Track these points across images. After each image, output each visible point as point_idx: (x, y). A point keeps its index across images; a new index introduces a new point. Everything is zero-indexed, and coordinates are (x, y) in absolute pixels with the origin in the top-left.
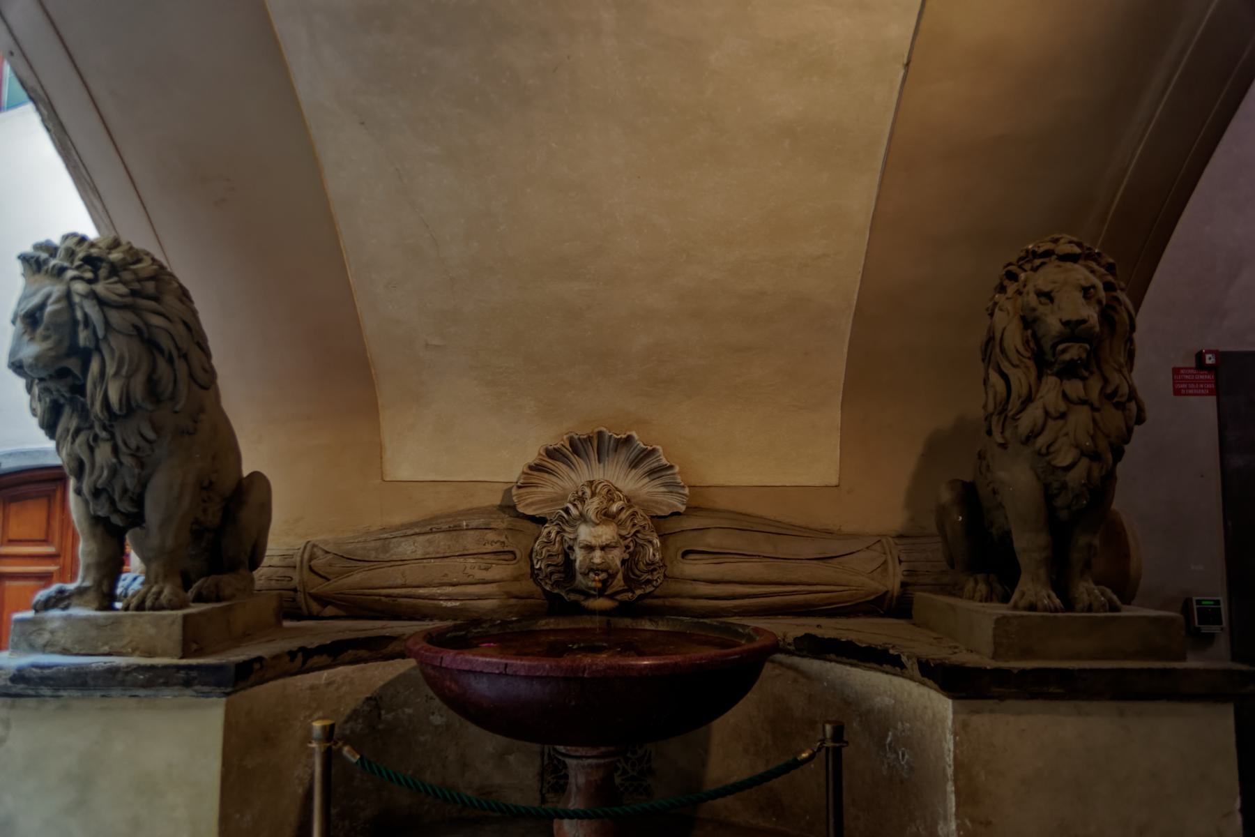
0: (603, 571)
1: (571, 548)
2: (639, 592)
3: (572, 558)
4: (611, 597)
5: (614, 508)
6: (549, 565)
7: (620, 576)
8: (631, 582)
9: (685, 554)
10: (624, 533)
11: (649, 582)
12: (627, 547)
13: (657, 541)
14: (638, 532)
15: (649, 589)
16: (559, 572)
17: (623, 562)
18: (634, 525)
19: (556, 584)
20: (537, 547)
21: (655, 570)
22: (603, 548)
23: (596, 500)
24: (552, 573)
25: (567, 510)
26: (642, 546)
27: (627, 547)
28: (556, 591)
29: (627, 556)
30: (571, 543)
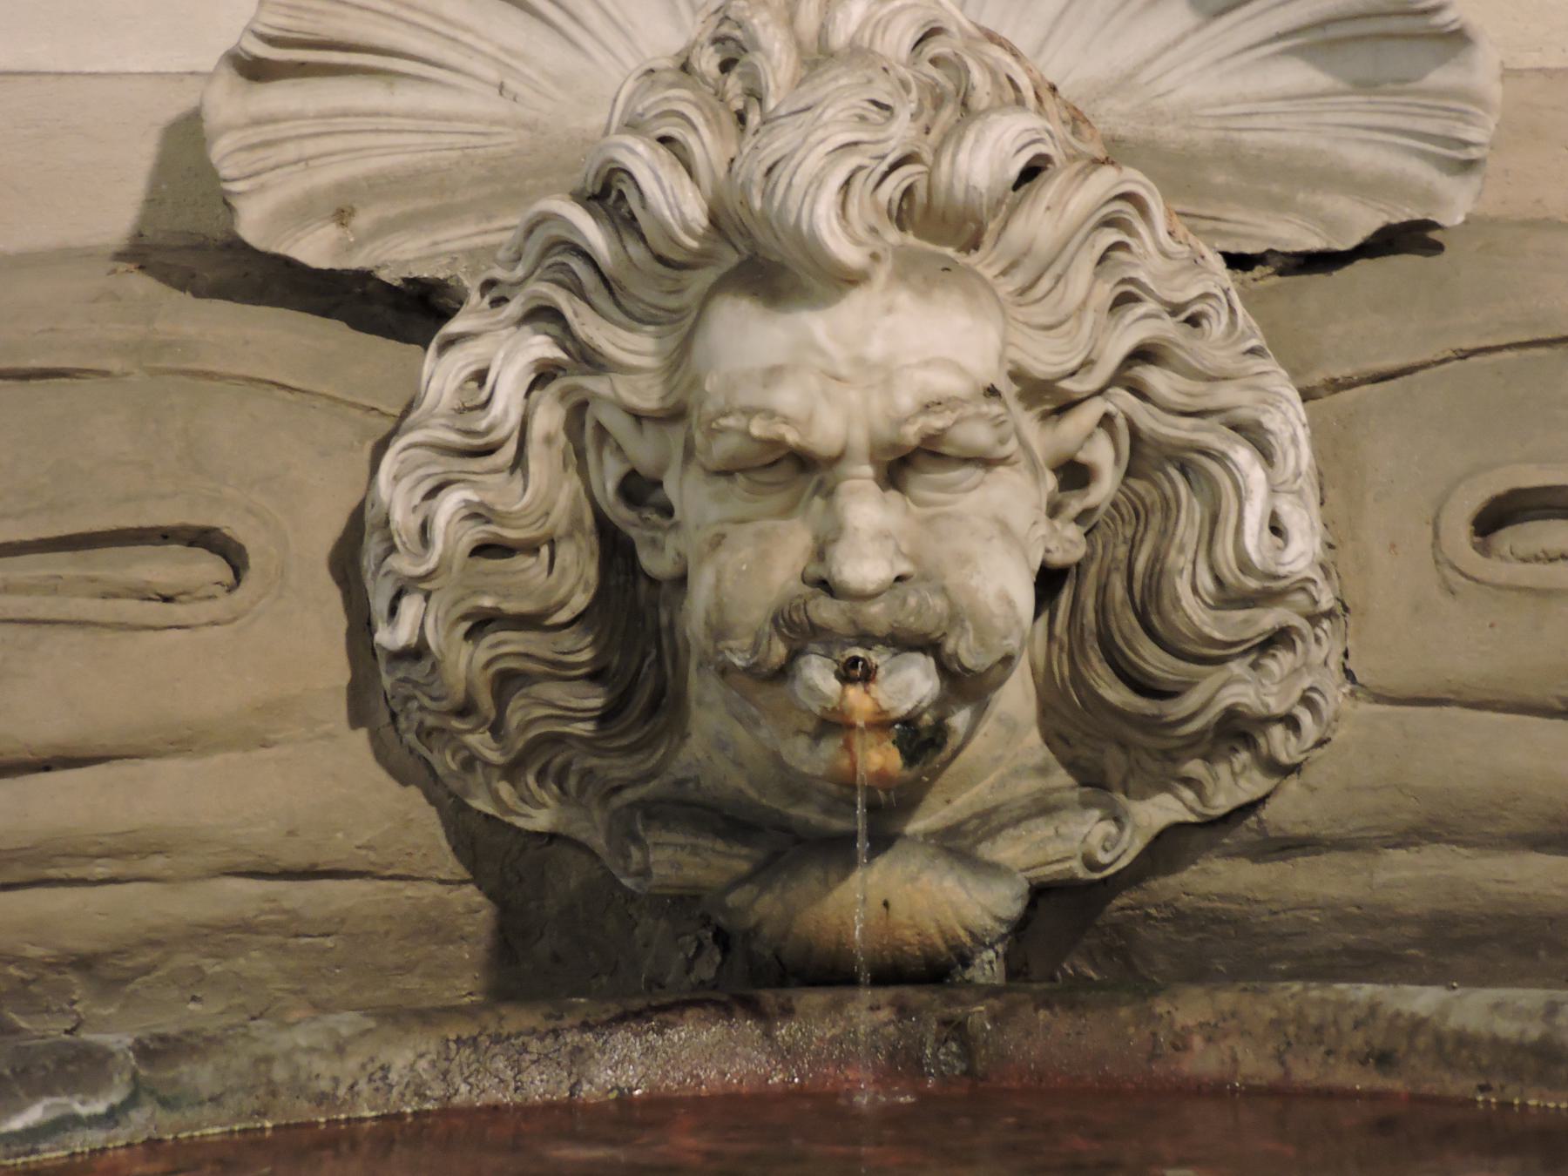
0: (904, 642)
1: (639, 489)
2: (1160, 811)
3: (656, 563)
4: (957, 846)
5: (983, 159)
6: (481, 624)
7: (1016, 697)
8: (1099, 743)
9: (1493, 519)
10: (1047, 357)
11: (1237, 731)
12: (1074, 474)
13: (1288, 420)
14: (1144, 354)
15: (1232, 783)
16: (558, 670)
17: (1049, 581)
18: (1123, 300)
19: (539, 757)
20: (397, 497)
21: (1280, 638)
22: (900, 466)
23: (842, 96)
24: (506, 682)
25: (608, 194)
26: (1186, 460)
27: (1074, 474)
28: (541, 820)
29: (1068, 544)
30: (643, 450)
